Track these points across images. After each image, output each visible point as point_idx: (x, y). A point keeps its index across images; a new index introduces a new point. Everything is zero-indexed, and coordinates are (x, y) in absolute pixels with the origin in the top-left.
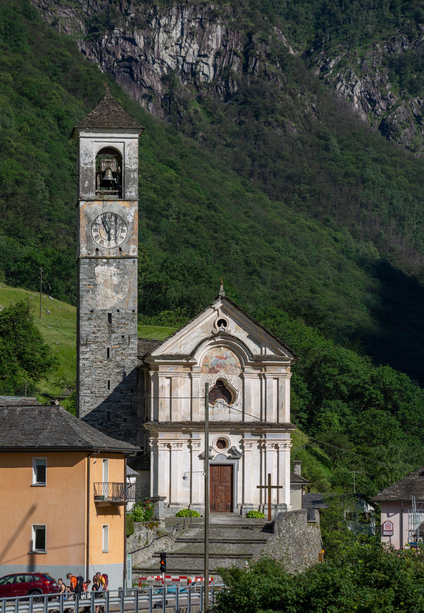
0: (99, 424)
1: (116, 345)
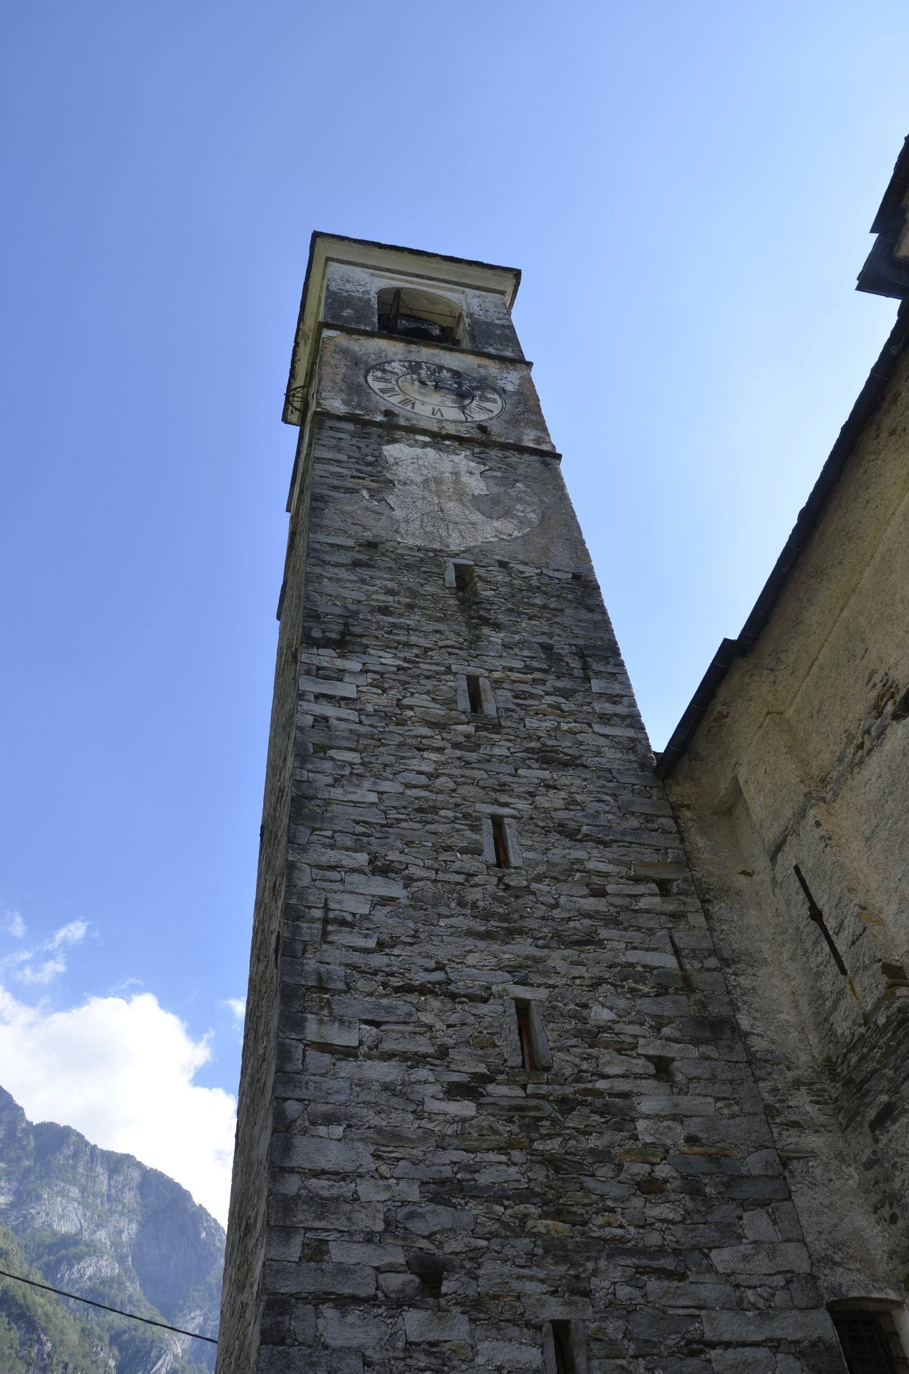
0: (454, 1091)
1: (511, 669)
